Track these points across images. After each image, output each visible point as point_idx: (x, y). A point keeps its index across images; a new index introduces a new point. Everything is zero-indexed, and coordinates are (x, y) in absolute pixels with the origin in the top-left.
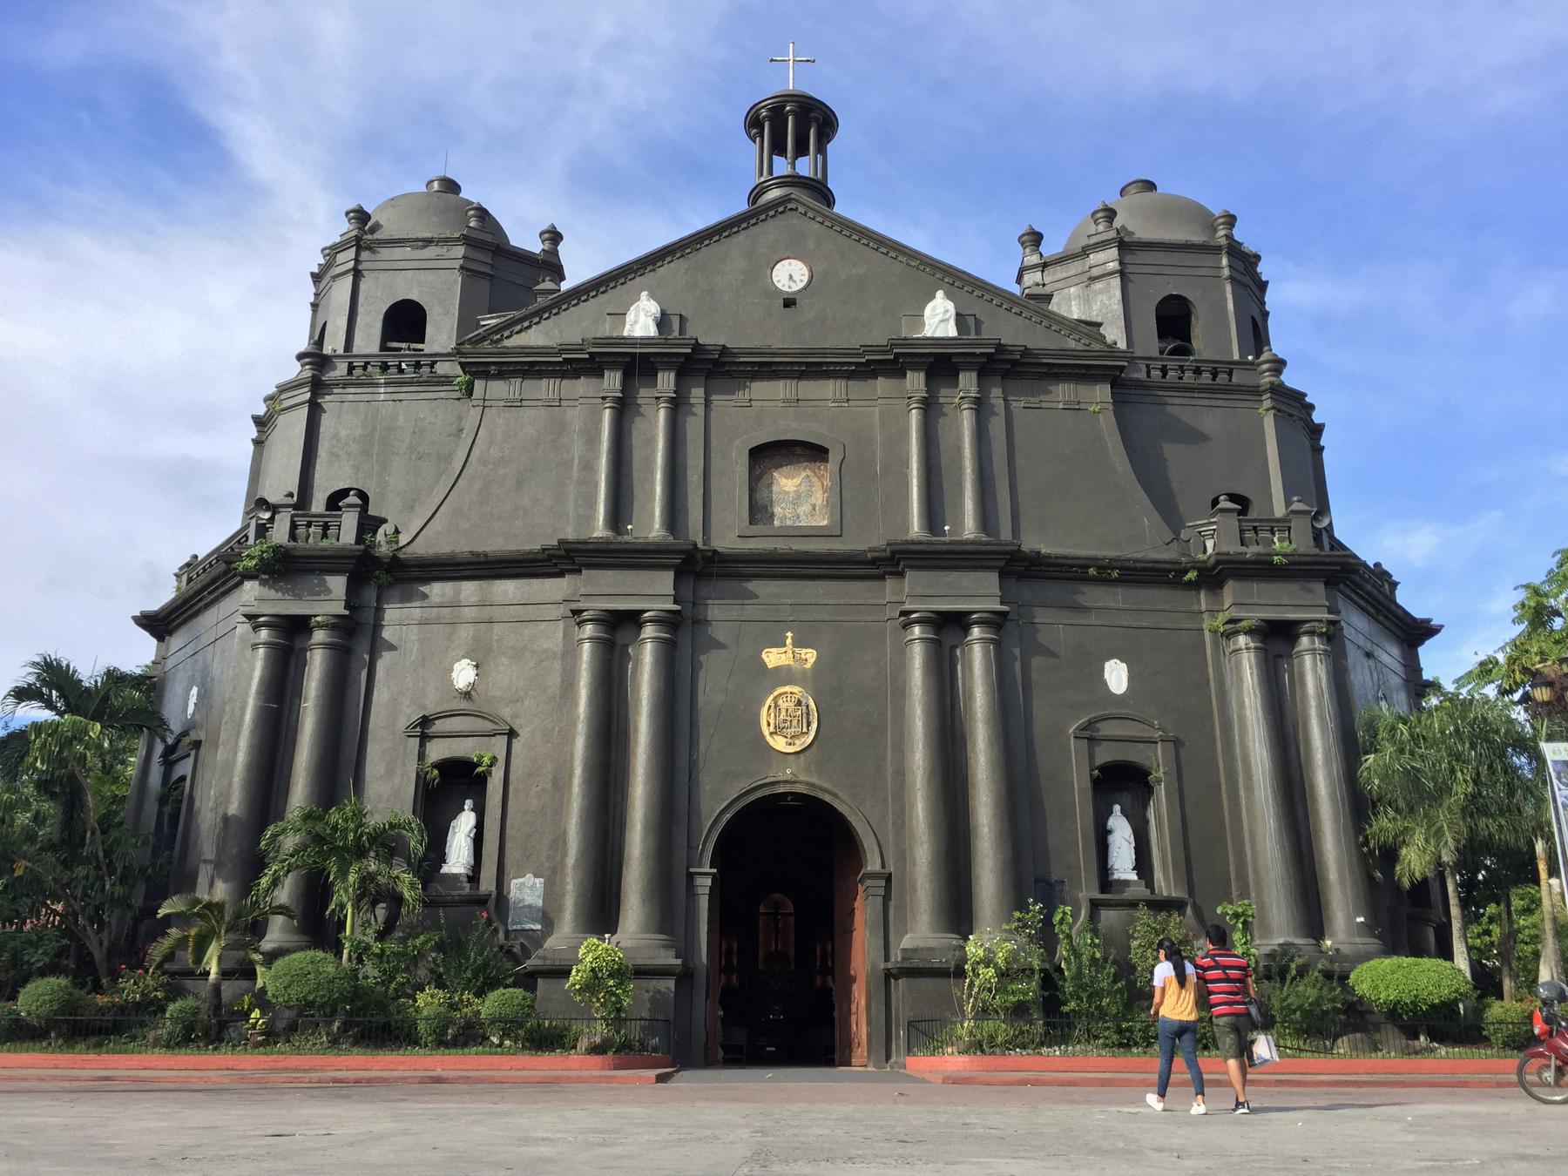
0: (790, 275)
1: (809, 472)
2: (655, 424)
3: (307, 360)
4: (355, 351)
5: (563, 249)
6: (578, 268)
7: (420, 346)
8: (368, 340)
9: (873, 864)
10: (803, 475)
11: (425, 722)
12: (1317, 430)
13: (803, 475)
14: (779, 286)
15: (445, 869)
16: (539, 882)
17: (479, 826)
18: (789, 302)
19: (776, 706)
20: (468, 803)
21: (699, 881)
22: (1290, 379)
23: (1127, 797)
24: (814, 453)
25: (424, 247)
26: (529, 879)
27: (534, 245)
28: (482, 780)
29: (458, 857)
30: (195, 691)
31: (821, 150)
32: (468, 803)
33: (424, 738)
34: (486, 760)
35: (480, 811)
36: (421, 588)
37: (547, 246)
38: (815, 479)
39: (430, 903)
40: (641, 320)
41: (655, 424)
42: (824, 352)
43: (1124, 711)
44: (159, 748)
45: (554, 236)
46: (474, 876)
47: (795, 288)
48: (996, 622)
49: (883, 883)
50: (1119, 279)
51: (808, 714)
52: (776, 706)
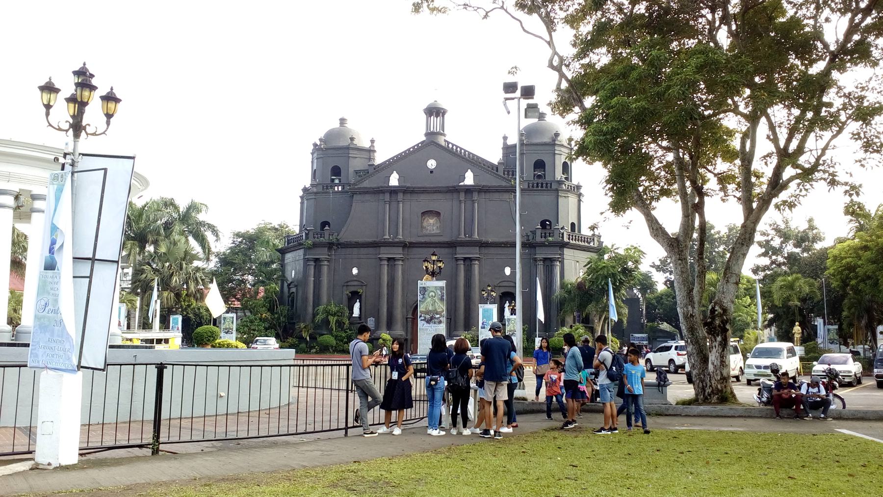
0: (432, 164)
5: (375, 144)
6: (379, 159)
11: (347, 282)
12: (580, 195)
15: (354, 315)
16: (374, 319)
17: (360, 306)
18: (432, 172)
20: (358, 300)
23: (509, 298)
24: (438, 214)
26: (372, 318)
27: (366, 145)
28: (361, 295)
29: (356, 312)
30: (293, 271)
31: (443, 116)
32: (358, 300)
34: (361, 291)
35: (360, 302)
39: (351, 324)
40: (394, 180)
42: (440, 187)
43: (509, 280)
44: (286, 285)
45: (372, 141)
46: (360, 317)
47: (433, 167)
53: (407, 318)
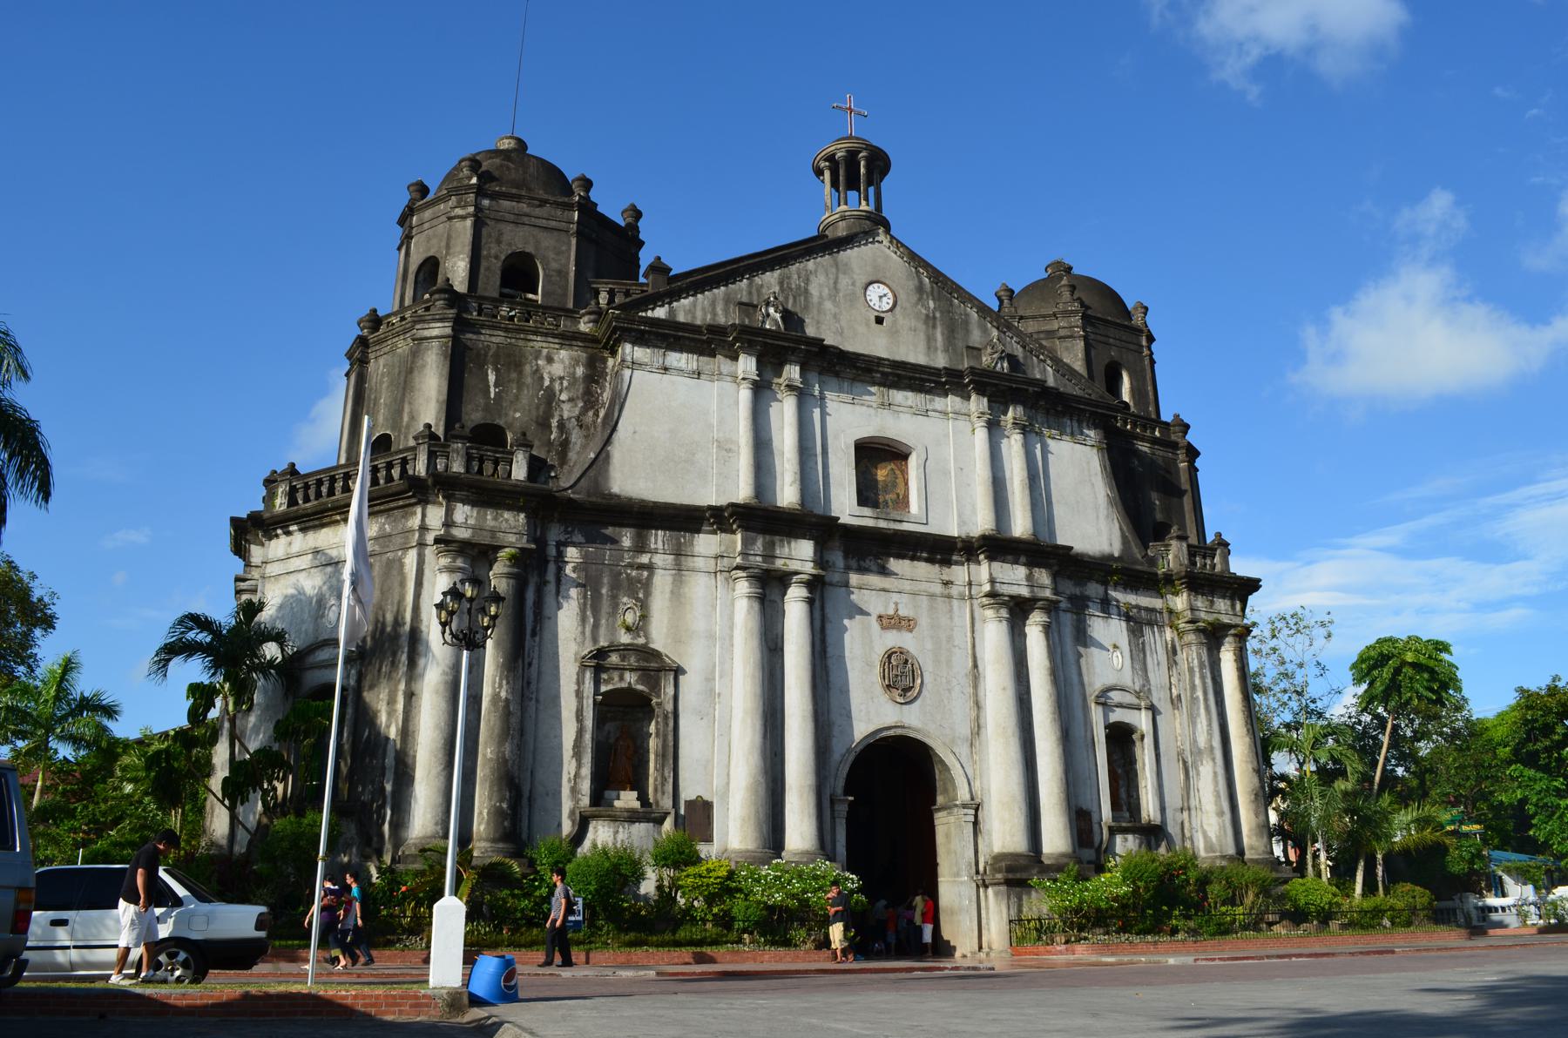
1: (892, 466)
2: (784, 413)
3: (443, 296)
4: (480, 292)
7: (530, 296)
8: (491, 285)
9: (963, 794)
10: (889, 468)
13: (889, 468)
14: (871, 304)
19: (890, 663)
21: (838, 807)
22: (1191, 437)
25: (540, 206)
33: (598, 670)
36: (603, 531)
37: (630, 220)
38: (898, 472)
41: (784, 413)
48: (1051, 608)
49: (973, 812)
50: (1082, 343)
51: (913, 671)
52: (890, 663)
53: (832, 802)
